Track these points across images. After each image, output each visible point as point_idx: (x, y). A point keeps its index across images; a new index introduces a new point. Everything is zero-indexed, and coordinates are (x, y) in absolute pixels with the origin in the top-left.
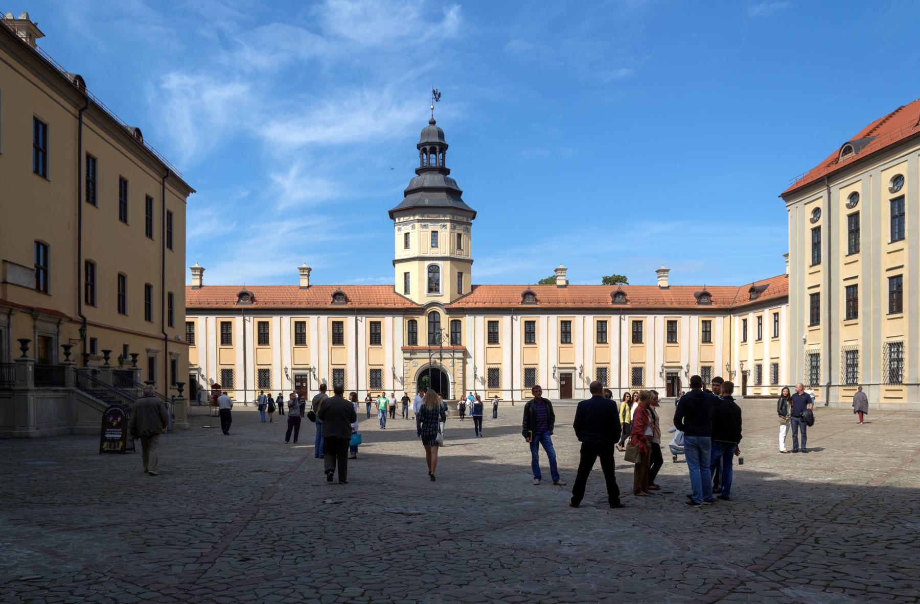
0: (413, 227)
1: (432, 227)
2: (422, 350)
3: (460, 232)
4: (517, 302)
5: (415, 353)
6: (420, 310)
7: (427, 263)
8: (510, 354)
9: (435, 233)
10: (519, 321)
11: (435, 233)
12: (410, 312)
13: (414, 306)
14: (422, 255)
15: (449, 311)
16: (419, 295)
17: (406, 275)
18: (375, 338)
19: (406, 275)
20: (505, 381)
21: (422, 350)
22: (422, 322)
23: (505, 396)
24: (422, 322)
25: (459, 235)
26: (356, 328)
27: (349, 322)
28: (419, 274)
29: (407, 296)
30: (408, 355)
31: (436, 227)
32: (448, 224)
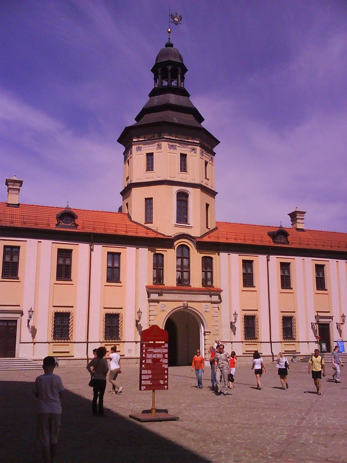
0: (159, 147)
1: (181, 149)
2: (171, 290)
3: (208, 160)
4: (268, 242)
5: (160, 294)
6: (167, 242)
7: (176, 189)
8: (267, 301)
9: (183, 157)
10: (275, 261)
11: (183, 157)
12: (156, 243)
13: (160, 236)
14: (169, 179)
15: (201, 246)
16: (165, 224)
17: (149, 201)
18: (113, 275)
19: (149, 201)
20: (263, 332)
21: (171, 290)
22: (170, 256)
23: (264, 350)
24: (170, 256)
25: (206, 163)
26: (89, 259)
27: (80, 251)
28: (166, 200)
29: (147, 225)
30: (154, 296)
31: (186, 150)
32: (198, 149)
